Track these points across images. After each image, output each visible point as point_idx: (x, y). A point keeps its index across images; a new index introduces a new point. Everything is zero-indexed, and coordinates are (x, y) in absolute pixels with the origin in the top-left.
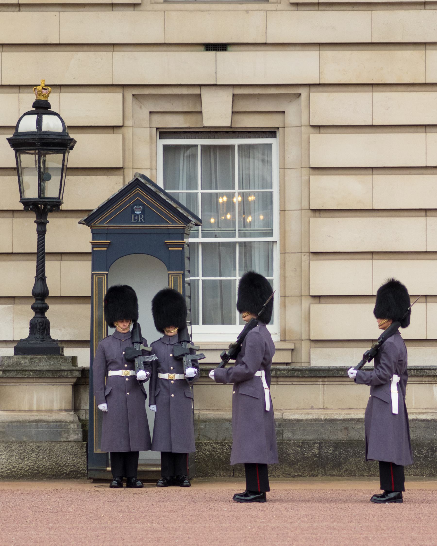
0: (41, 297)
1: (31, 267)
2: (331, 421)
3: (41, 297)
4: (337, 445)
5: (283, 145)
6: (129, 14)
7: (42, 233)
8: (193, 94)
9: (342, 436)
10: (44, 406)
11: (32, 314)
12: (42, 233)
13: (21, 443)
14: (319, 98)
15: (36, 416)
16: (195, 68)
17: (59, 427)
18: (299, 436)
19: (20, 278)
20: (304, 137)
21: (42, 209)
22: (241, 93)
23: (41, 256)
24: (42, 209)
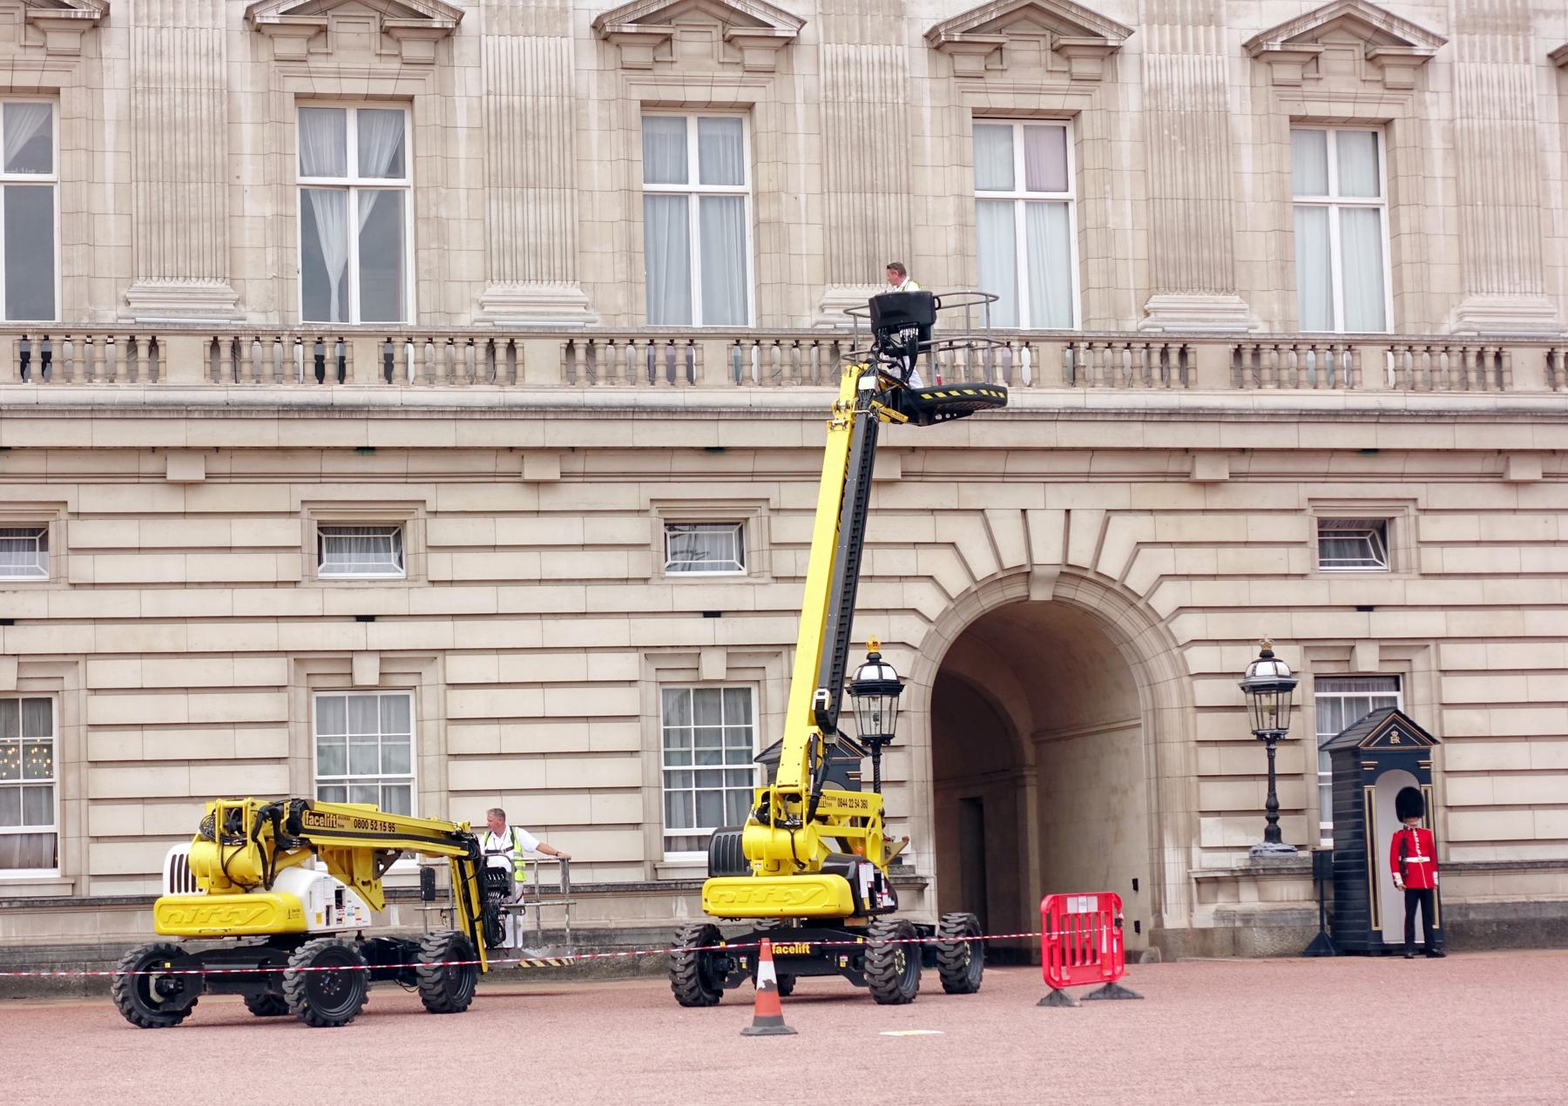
0: (1272, 811)
1: (1266, 783)
2: (1503, 904)
3: (1272, 811)
4: (1510, 924)
5: (420, 701)
6: (1302, 582)
7: (1271, 759)
8: (1349, 646)
9: (1512, 916)
10: (1293, 897)
11: (1266, 823)
12: (1271, 759)
13: (1281, 928)
14: (1445, 648)
15: (1289, 905)
16: (1354, 625)
17: (1310, 912)
18: (1480, 917)
19: (1257, 795)
20: (1434, 680)
21: (1270, 740)
22: (1387, 645)
23: (1272, 777)
24: (1270, 740)
